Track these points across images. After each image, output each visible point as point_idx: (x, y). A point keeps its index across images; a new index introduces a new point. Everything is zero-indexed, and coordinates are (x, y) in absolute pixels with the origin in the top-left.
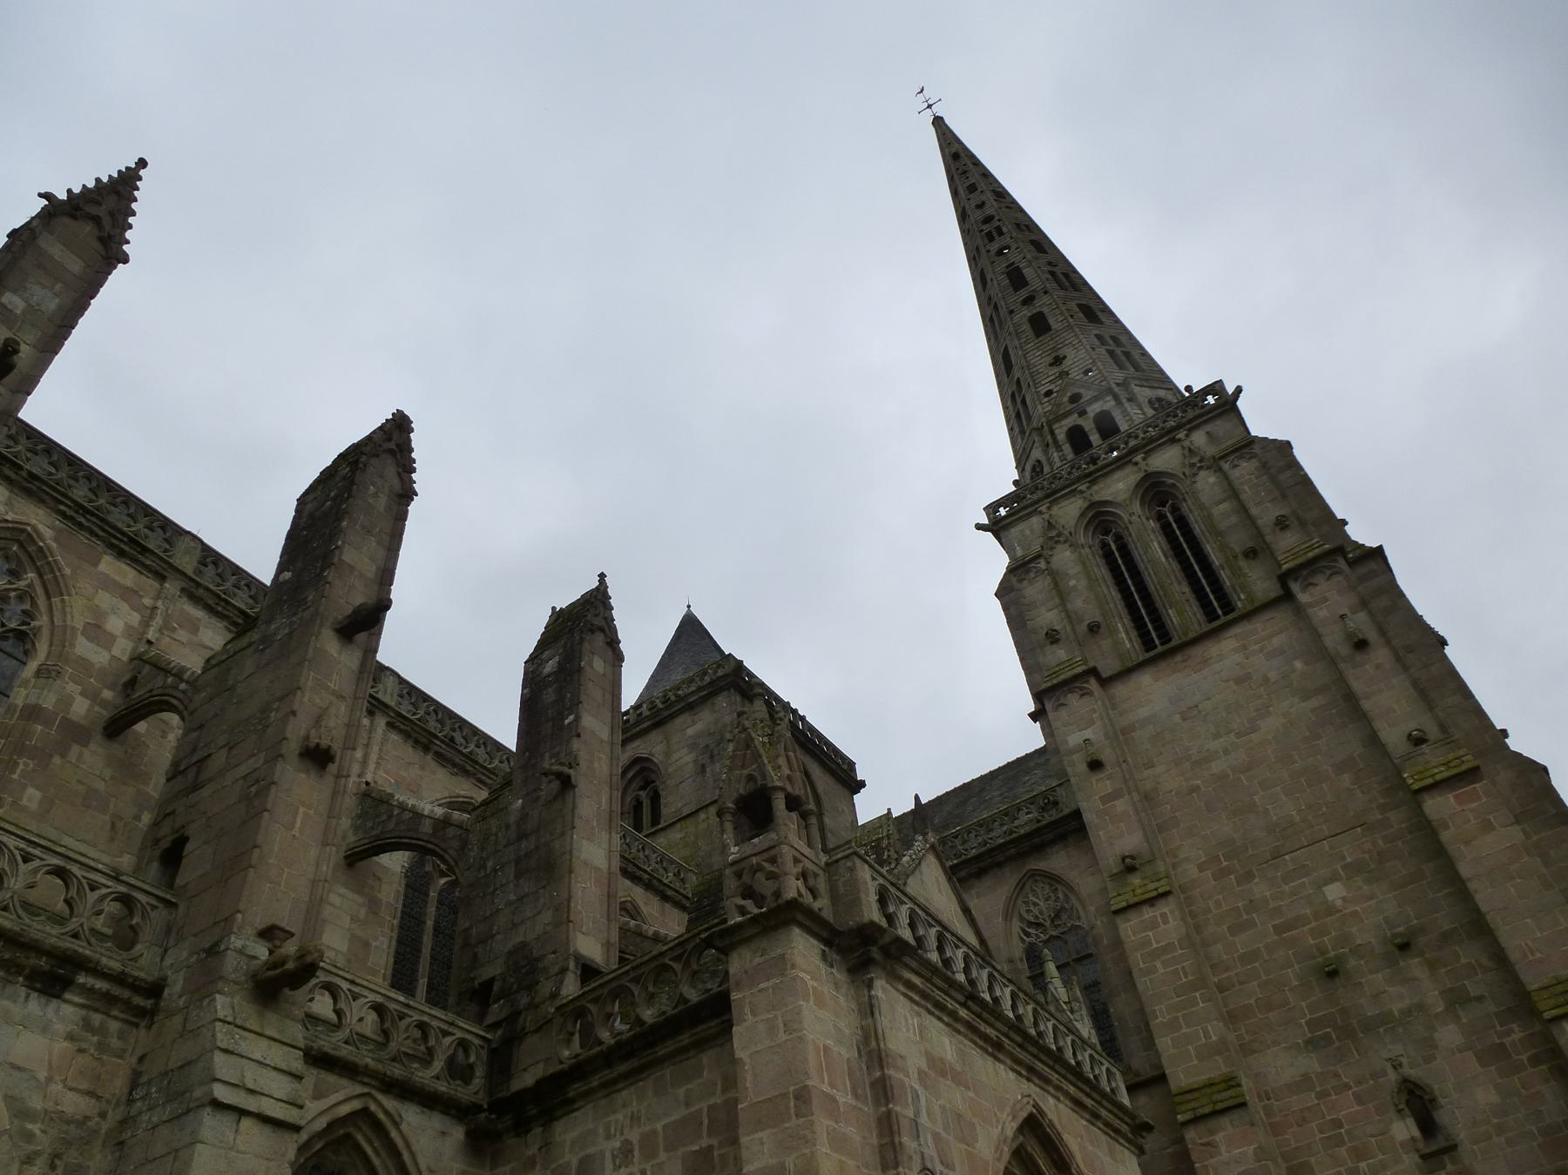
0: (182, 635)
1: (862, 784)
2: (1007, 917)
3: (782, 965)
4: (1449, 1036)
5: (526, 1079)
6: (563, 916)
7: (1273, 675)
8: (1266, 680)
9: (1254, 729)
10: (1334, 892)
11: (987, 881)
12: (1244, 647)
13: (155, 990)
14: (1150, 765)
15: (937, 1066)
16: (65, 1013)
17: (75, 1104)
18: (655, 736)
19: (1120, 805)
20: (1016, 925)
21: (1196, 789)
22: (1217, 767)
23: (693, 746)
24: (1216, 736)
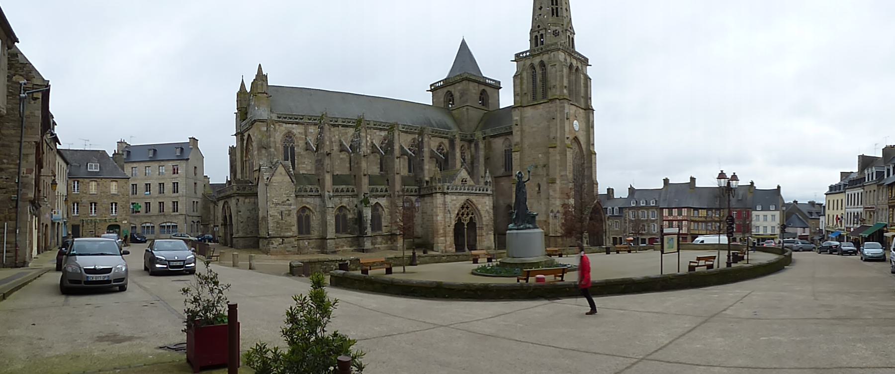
0: (375, 135)
2: (503, 144)
3: (436, 196)
4: (545, 179)
5: (422, 193)
6: (424, 177)
10: (540, 155)
11: (501, 137)
13: (391, 195)
16: (385, 198)
17: (388, 204)
19: (518, 133)
20: (504, 146)
22: (534, 129)
23: (459, 92)
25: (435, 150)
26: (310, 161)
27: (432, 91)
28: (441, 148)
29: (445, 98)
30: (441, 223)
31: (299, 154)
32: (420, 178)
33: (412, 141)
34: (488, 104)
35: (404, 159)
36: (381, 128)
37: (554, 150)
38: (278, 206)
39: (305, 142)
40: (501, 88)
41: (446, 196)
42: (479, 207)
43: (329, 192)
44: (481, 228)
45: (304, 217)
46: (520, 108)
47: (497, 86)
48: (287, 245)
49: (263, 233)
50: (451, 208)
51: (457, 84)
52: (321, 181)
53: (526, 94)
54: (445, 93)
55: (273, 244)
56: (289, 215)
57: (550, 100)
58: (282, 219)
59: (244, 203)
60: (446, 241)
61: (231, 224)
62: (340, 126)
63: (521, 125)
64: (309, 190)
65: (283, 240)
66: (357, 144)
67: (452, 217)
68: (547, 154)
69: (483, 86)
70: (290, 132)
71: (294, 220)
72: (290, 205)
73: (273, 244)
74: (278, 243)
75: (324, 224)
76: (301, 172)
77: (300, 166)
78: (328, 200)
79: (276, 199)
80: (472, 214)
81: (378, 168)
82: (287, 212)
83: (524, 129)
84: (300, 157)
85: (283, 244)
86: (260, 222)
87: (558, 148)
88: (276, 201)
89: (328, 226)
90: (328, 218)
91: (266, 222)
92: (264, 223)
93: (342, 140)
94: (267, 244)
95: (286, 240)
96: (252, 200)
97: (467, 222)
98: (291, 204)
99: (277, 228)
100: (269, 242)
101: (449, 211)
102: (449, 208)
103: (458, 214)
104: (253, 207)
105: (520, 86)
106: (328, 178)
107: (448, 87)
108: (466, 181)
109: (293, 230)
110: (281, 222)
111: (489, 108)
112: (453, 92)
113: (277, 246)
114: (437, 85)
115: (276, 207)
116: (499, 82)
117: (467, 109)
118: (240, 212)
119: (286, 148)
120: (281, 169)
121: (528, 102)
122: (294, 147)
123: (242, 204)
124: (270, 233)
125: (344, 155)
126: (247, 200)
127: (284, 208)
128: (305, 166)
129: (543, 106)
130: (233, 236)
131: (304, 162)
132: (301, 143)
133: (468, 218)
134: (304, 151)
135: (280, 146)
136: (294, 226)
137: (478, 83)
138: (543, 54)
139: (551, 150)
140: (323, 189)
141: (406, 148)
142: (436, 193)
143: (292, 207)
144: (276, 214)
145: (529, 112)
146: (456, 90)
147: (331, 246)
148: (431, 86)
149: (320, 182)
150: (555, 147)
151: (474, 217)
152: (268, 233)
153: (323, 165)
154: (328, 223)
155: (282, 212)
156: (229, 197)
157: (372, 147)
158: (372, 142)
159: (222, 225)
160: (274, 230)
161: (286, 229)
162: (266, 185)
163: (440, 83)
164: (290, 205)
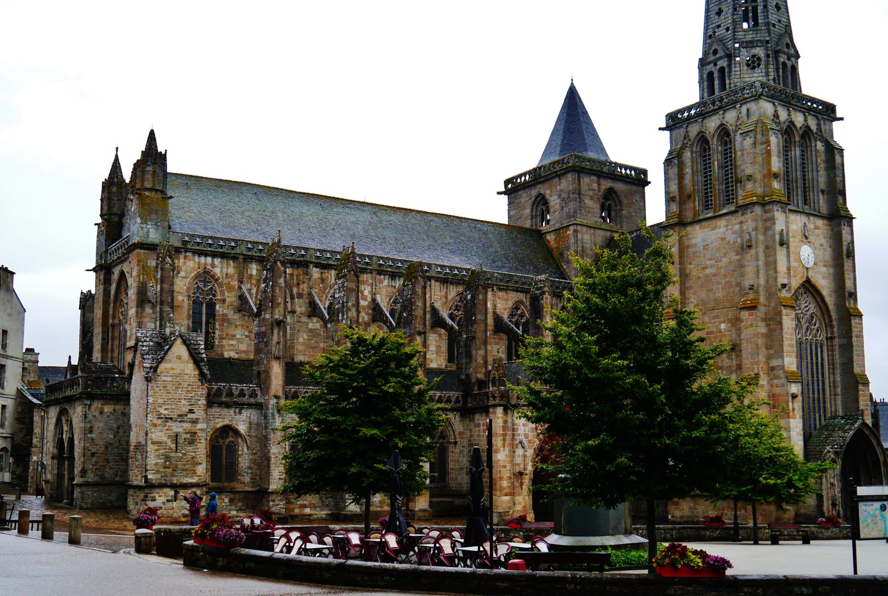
1: (650, 183)
3: (495, 413)
7: (731, 242)
8: (729, 241)
9: (720, 261)
10: (723, 326)
12: (727, 226)
14: (690, 264)
18: (546, 185)
21: (699, 278)
22: (708, 271)
23: (560, 196)
24: (710, 259)
25: (505, 316)
26: (246, 333)
27: (508, 195)
28: (519, 312)
29: (534, 210)
30: (505, 467)
31: (225, 319)
32: (468, 376)
33: (458, 298)
34: (621, 217)
35: (440, 335)
36: (393, 272)
37: (749, 315)
38: (170, 423)
39: (239, 294)
40: (648, 183)
43: (277, 397)
46: (677, 229)
47: (639, 179)
49: (136, 479)
50: (526, 436)
51: (556, 180)
52: (263, 376)
53: (690, 196)
54: (533, 199)
55: (154, 500)
56: (192, 442)
57: (741, 207)
58: (177, 449)
59: (101, 413)
60: (514, 504)
61: (71, 458)
63: (680, 263)
64: (236, 393)
65: (176, 493)
66: (339, 303)
67: (528, 454)
68: (736, 322)
69: (609, 181)
70: (206, 272)
71: (201, 450)
72: (195, 422)
73: (154, 500)
74: (164, 499)
75: (263, 463)
76: (226, 355)
77: (225, 342)
78: (273, 415)
79: (166, 409)
82: (188, 436)
83: (688, 272)
84: (225, 324)
85: (175, 500)
86: (132, 454)
87: (761, 311)
88: (166, 412)
89: (272, 467)
90: (272, 451)
91: (142, 455)
92: (140, 457)
93: (314, 291)
94: (142, 500)
95: (182, 493)
96: (120, 408)
98: (196, 419)
99: (165, 468)
100: (146, 496)
101: (521, 442)
102: (522, 437)
104: (120, 422)
105: (677, 181)
106: (277, 371)
107: (539, 186)
109: (198, 474)
111: (621, 227)
112: (547, 197)
113: (164, 503)
114: (519, 180)
115: (165, 426)
116: (645, 172)
117: (575, 231)
118: (91, 432)
119: (196, 304)
120: (179, 349)
121: (695, 215)
122: (215, 304)
123: (97, 414)
124: (149, 477)
125: (315, 324)
126: (108, 409)
127: (182, 427)
128: (234, 342)
129: (728, 220)
130: (75, 482)
131: (234, 336)
132: (231, 298)
134: (235, 312)
135: (186, 299)
136: (200, 464)
137: (599, 177)
138: (725, 111)
139: (744, 315)
140: (268, 388)
141: (445, 315)
142: (495, 406)
143: (199, 426)
144: (165, 439)
145: (699, 235)
146: (554, 195)
148: (507, 182)
149: (262, 379)
150: (754, 308)
152: (146, 477)
153: (267, 344)
154: (273, 460)
155: (177, 436)
156: (71, 400)
157: (374, 309)
158: (374, 300)
159: (53, 458)
160: (158, 472)
161: (183, 470)
162: (148, 380)
163: (523, 178)
164: (195, 422)
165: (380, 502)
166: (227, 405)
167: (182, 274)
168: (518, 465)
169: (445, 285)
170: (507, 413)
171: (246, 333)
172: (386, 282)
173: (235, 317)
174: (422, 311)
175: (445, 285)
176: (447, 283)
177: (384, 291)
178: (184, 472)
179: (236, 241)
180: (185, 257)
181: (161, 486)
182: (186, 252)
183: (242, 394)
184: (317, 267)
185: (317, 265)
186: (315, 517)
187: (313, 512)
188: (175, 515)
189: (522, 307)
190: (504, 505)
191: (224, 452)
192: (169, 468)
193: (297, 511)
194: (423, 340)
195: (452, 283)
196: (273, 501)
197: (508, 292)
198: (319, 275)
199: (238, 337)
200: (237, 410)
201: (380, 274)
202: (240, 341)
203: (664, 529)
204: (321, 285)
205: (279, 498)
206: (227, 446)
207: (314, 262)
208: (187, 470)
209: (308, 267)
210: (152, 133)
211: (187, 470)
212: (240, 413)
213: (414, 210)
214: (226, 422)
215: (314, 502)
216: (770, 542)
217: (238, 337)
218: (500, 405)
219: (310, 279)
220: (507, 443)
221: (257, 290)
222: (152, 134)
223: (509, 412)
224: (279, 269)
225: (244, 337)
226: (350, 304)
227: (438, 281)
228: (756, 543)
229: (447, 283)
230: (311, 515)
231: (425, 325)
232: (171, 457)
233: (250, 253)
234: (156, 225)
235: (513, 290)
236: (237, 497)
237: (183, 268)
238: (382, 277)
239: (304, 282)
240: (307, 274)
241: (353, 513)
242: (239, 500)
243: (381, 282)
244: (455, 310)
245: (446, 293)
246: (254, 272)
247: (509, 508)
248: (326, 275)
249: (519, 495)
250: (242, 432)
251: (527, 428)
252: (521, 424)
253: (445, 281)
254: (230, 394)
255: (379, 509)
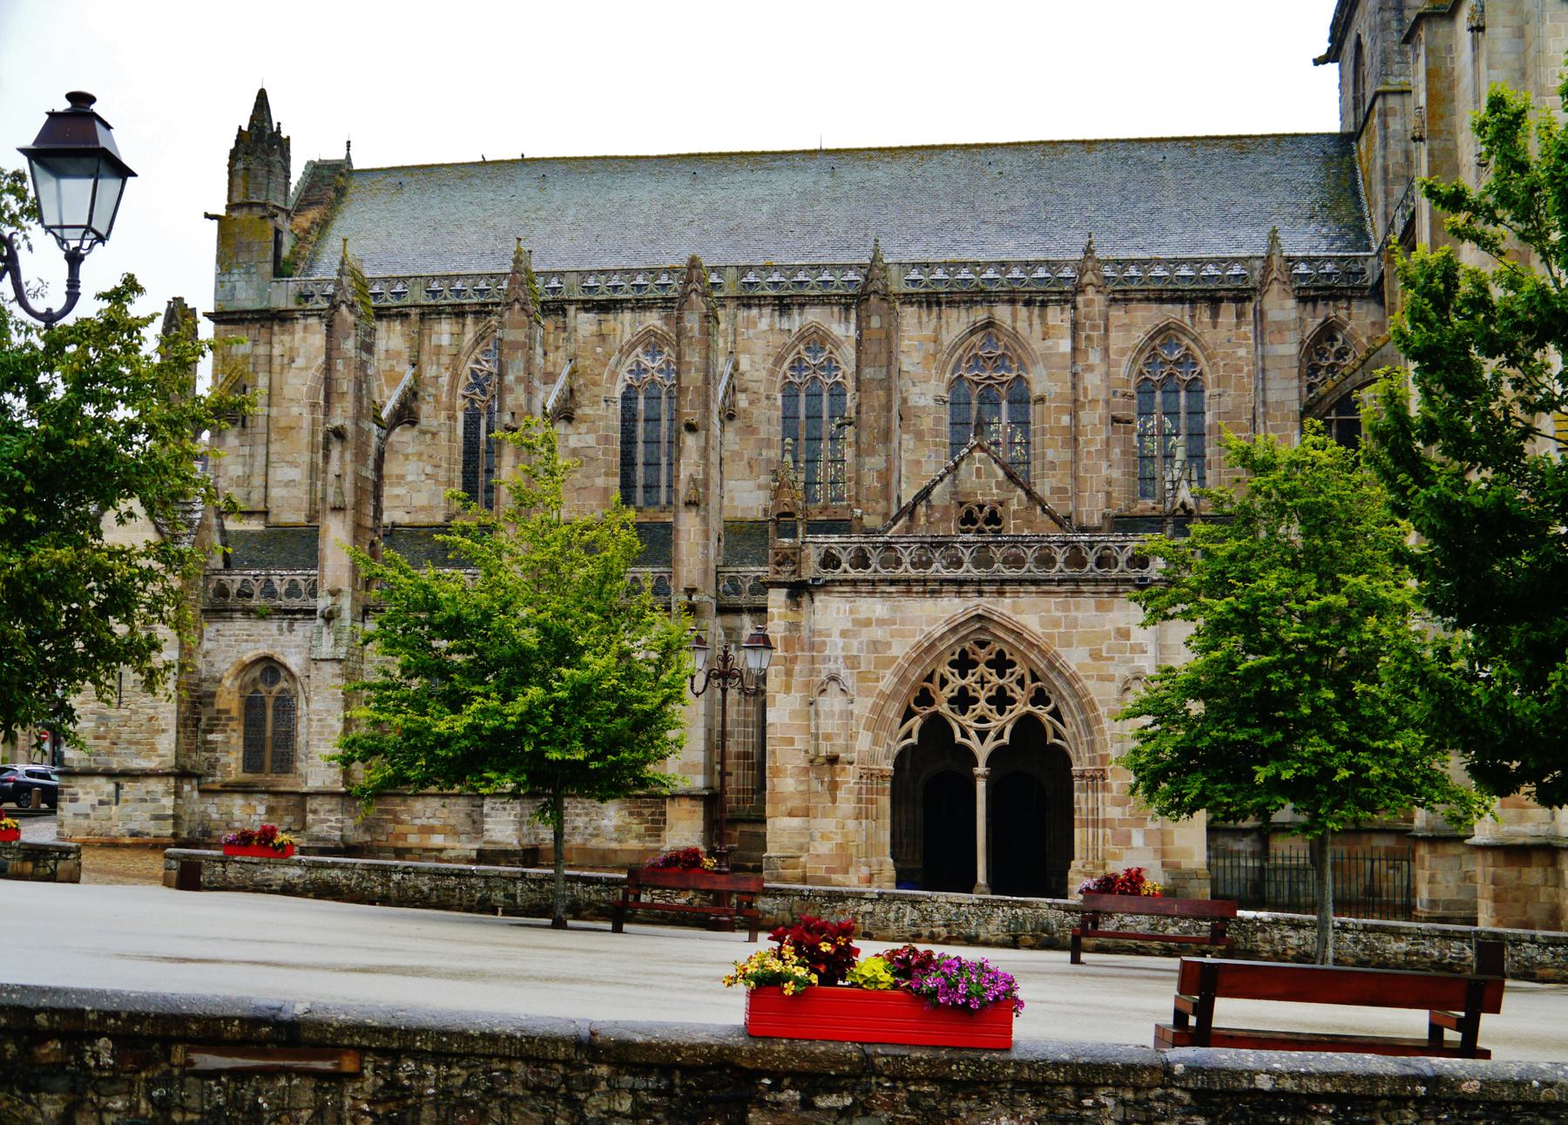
15: (868, 623)
26: (429, 470)
36: (781, 298)
41: (820, 599)
42: (1074, 658)
44: (1097, 779)
45: (270, 702)
48: (128, 809)
55: (74, 800)
62: (572, 310)
65: (118, 786)
67: (856, 709)
73: (74, 800)
80: (1040, 698)
81: (760, 487)
95: (129, 789)
97: (990, 744)
99: (97, 738)
103: (925, 698)
108: (994, 518)
110: (112, 712)
113: (93, 806)
133: (1003, 722)
147: (325, 826)
151: (1056, 713)
161: (130, 743)
165: (618, 829)
166: (263, 616)
167: (300, 362)
168: (828, 737)
169: (935, 309)
170: (799, 605)
171: (429, 470)
172: (764, 324)
173: (403, 439)
174: (701, 376)
175: (935, 309)
176: (939, 304)
177: (759, 346)
178: (134, 749)
179: (404, 279)
180: (305, 328)
181: (89, 773)
182: (306, 317)
183: (293, 591)
184: (587, 310)
185: (587, 306)
186: (452, 854)
187: (449, 844)
188: (114, 832)
189: (1186, 341)
190: (786, 840)
191: (270, 713)
192: (104, 738)
193: (413, 840)
194: (702, 443)
195: (951, 303)
196: (315, 812)
197: (1133, 305)
198: (595, 328)
199: (410, 478)
200: (285, 624)
201: (749, 306)
202: (414, 487)
203: (486, 878)
204: (599, 350)
205: (328, 807)
206: (278, 698)
207: (577, 301)
208: (137, 743)
209: (565, 312)
210: (262, 96)
211: (137, 743)
212: (291, 630)
213: (954, 146)
214: (263, 650)
215: (452, 822)
216: (609, 926)
217: (410, 478)
218: (780, 585)
219: (568, 340)
220: (797, 680)
221: (455, 377)
222: (262, 96)
223: (805, 600)
224: (344, 321)
225: (423, 477)
226: (510, 378)
227: (912, 304)
228: (559, 925)
229: (939, 304)
230: (440, 850)
231: (707, 406)
232: (107, 718)
233: (432, 302)
234: (248, 272)
235: (1148, 299)
236: (283, 802)
237: (302, 351)
238: (755, 312)
239: (557, 348)
240: (565, 329)
241: (498, 847)
242: (287, 811)
243: (752, 324)
244: (970, 369)
245: (938, 331)
246: (445, 340)
247: (801, 848)
248: (605, 328)
249: (825, 815)
250: (294, 669)
251: (855, 643)
252: (836, 633)
253: (931, 300)
254: (270, 592)
255: (614, 845)
